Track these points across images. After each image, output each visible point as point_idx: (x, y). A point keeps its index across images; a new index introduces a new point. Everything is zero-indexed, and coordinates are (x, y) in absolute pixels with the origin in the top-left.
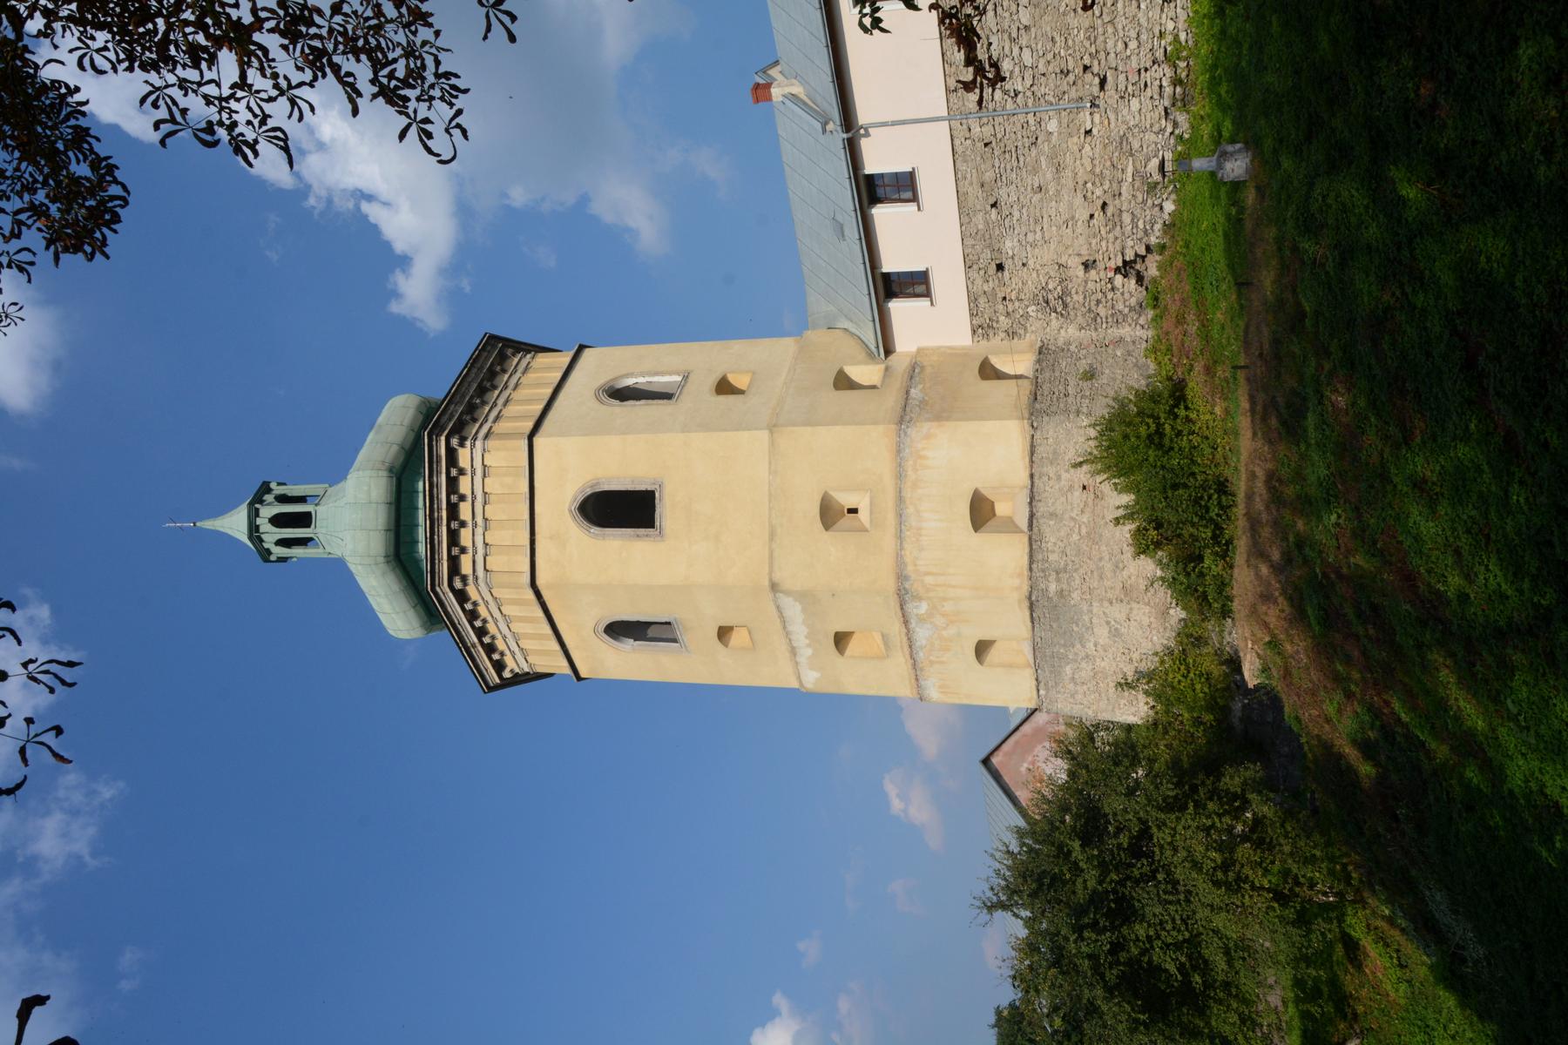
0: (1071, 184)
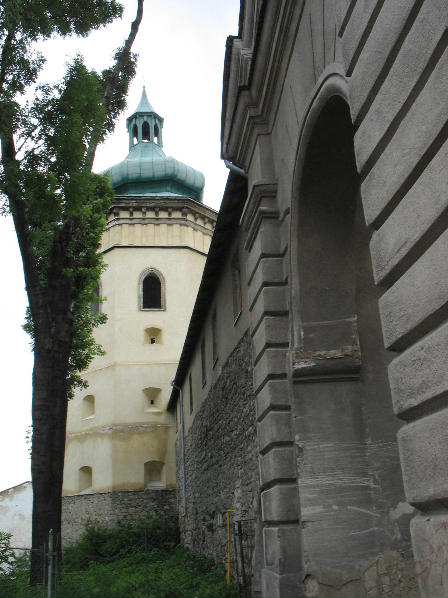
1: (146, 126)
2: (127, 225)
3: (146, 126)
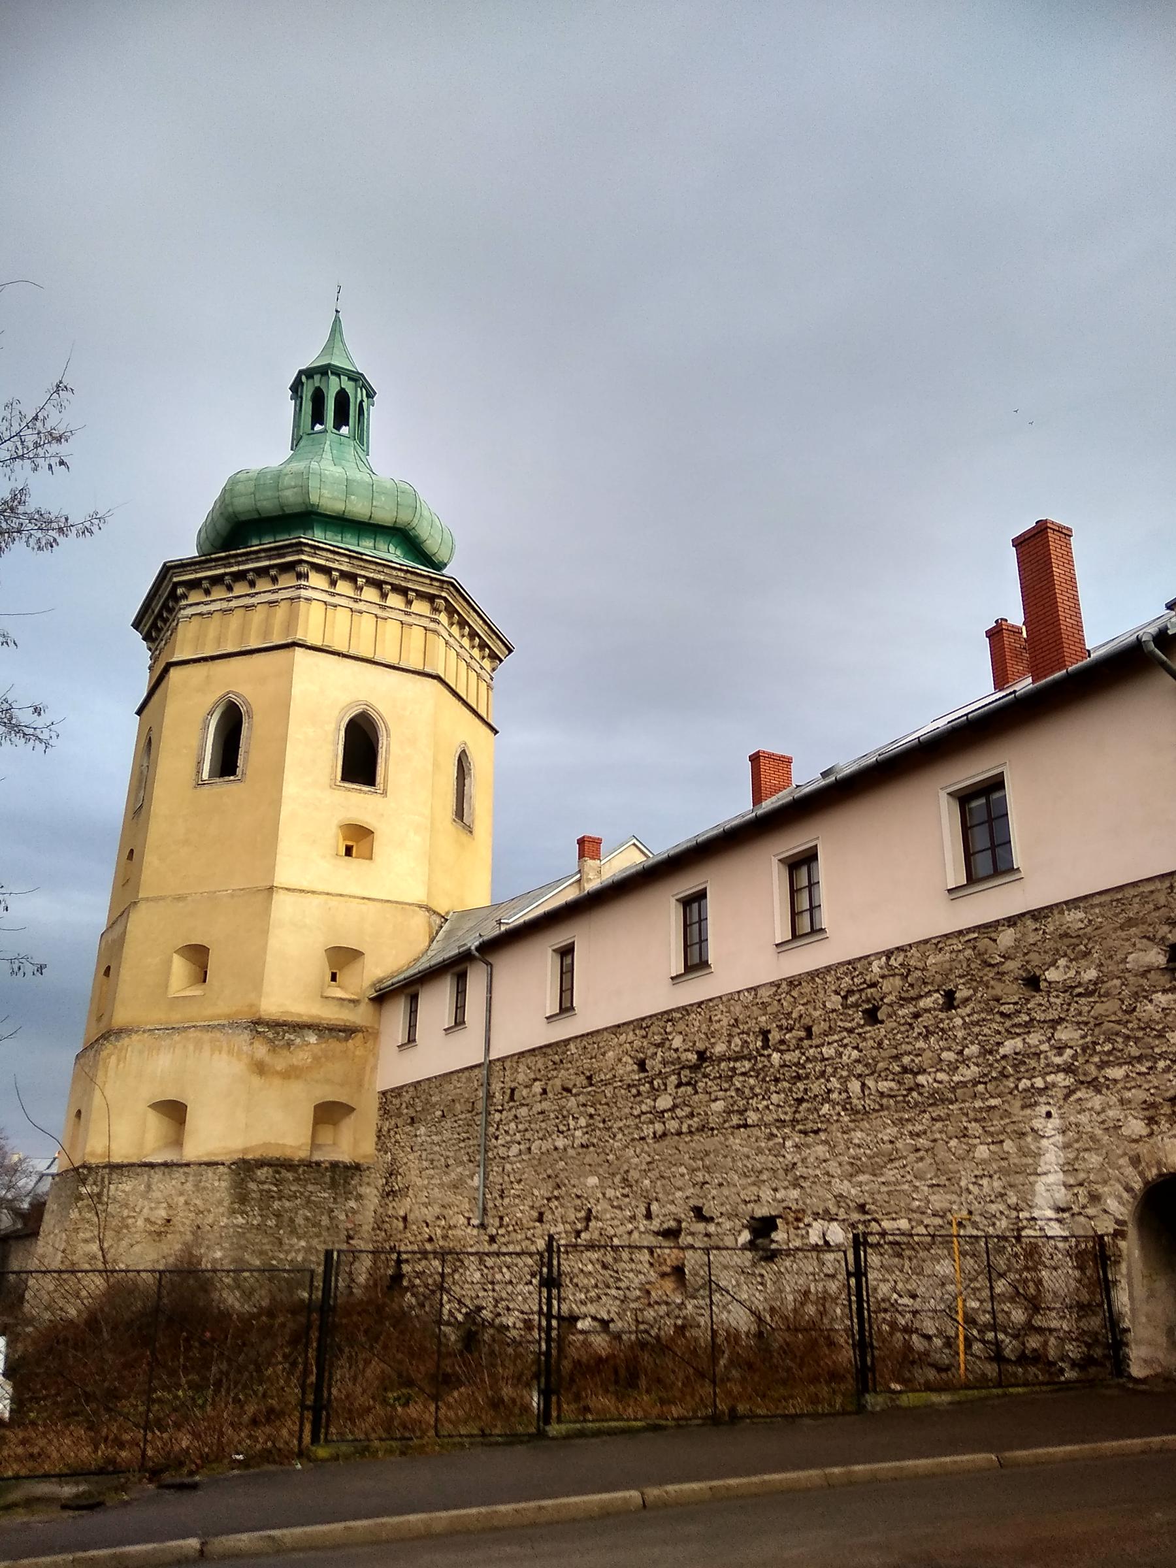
0: (447, 1200)
1: (342, 399)
3: (342, 399)
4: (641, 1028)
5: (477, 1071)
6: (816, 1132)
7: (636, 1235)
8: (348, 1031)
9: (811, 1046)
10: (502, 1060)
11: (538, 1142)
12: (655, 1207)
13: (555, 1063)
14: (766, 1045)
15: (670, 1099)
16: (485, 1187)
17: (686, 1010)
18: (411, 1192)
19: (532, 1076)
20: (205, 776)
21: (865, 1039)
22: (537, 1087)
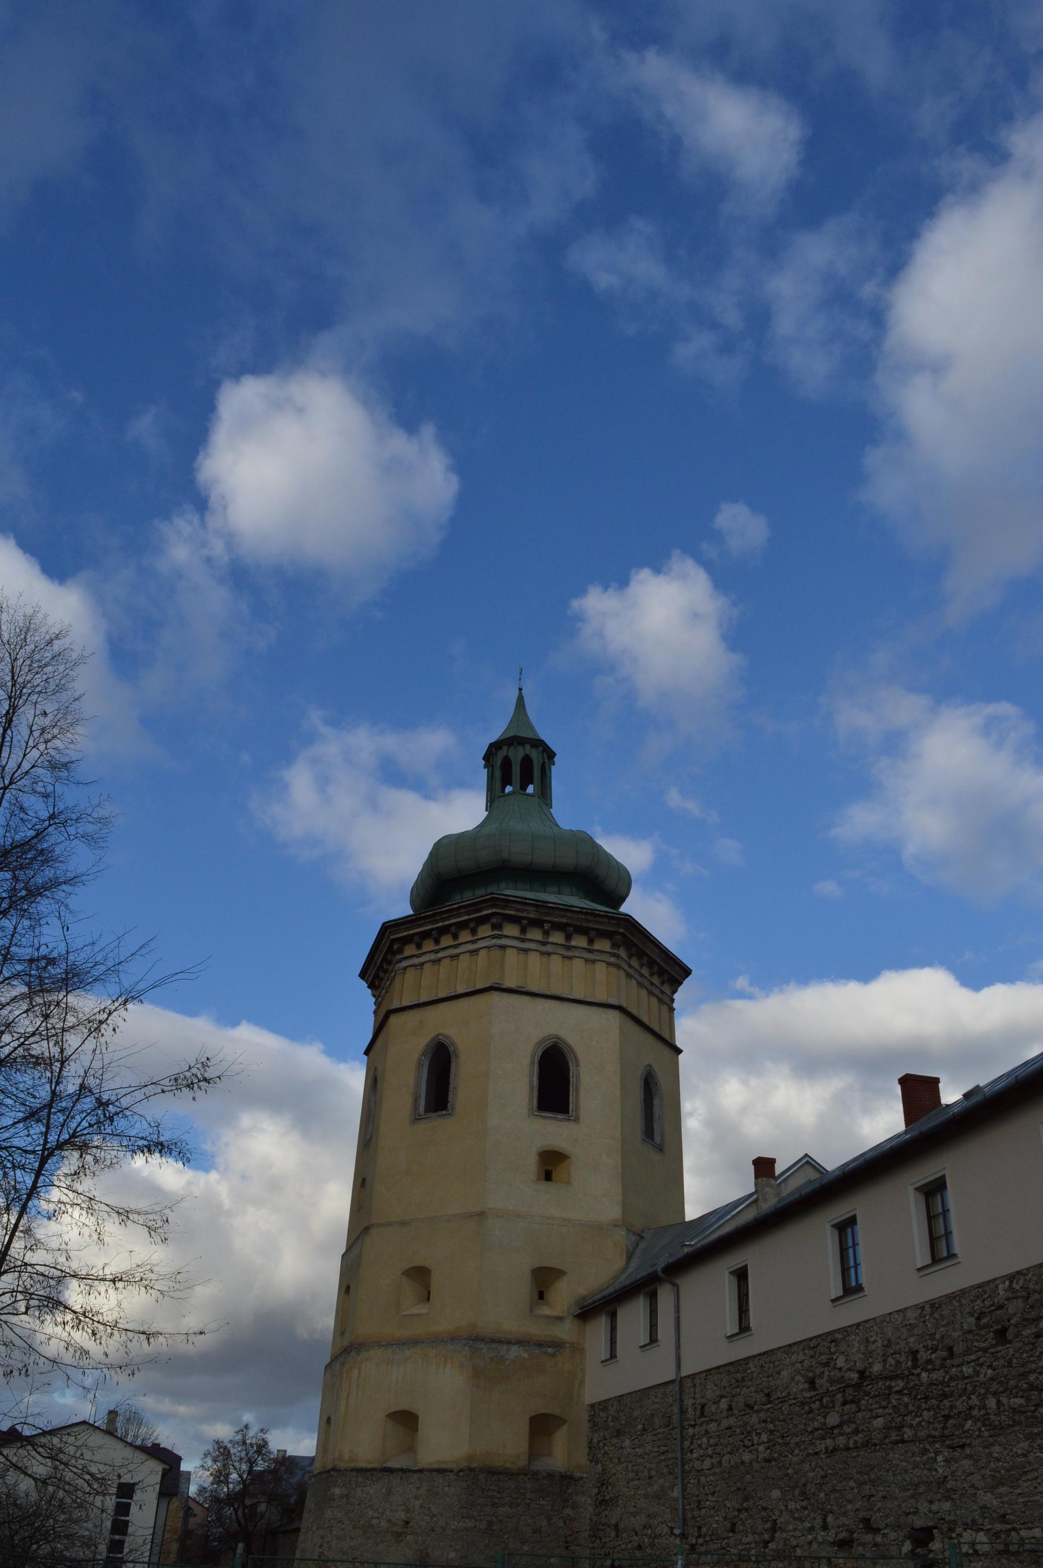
1: (527, 763)
2: (515, 951)
3: (527, 763)
4: (810, 1348)
5: (671, 1387)
6: (963, 1447)
7: (815, 1546)
8: (557, 1345)
9: (953, 1366)
10: (693, 1376)
11: (727, 1456)
12: (830, 1518)
13: (738, 1381)
14: (915, 1366)
15: (838, 1416)
16: (684, 1498)
17: (845, 1330)
18: (620, 1502)
19: (719, 1393)
20: (422, 1109)
21: (997, 1359)
22: (724, 1404)
